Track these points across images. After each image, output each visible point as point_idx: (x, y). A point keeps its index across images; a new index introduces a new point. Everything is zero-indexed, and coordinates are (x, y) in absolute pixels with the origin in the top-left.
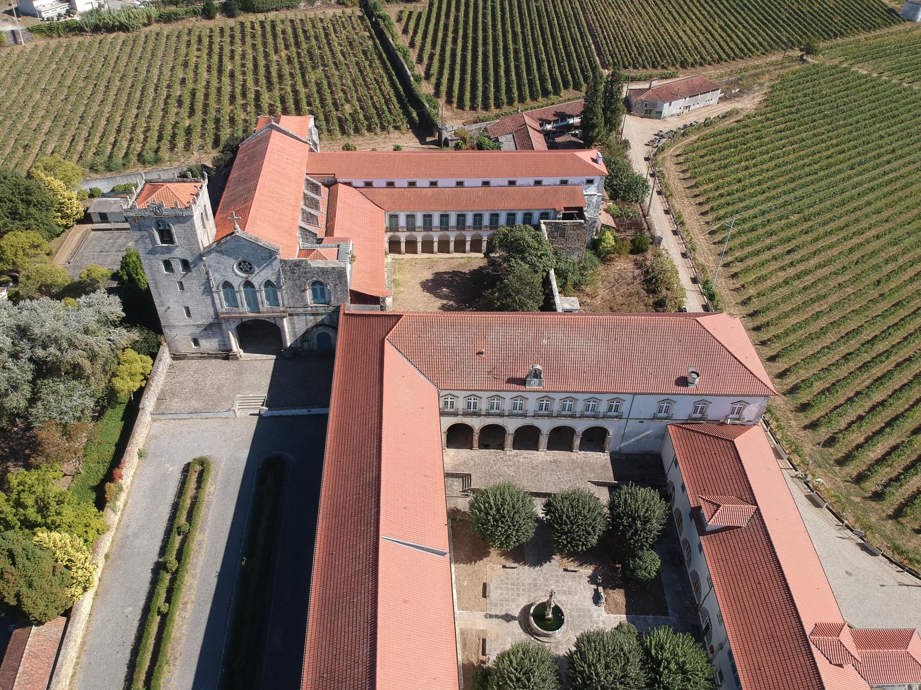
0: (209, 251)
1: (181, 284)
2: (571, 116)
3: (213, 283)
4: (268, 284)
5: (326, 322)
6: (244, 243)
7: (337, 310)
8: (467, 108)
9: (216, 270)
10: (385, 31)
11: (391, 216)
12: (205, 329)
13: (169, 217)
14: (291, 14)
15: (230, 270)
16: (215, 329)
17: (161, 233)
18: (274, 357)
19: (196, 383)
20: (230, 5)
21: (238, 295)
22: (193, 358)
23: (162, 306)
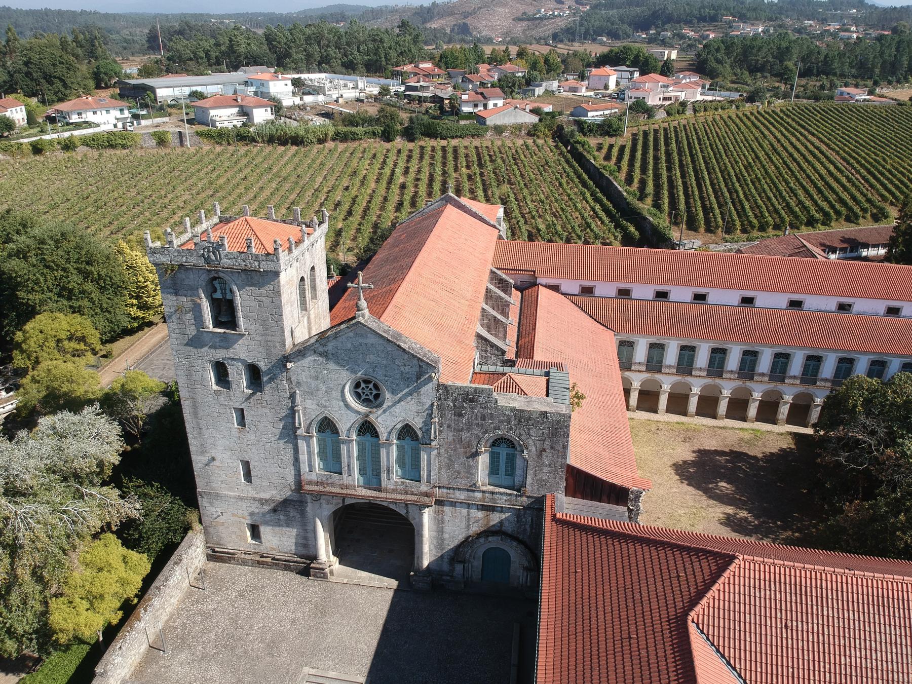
0: (301, 352)
1: (241, 413)
2: (866, 246)
3: (301, 419)
4: (406, 432)
5: (508, 528)
6: (372, 340)
7: (537, 506)
8: (702, 230)
9: (310, 393)
10: (585, 154)
11: (622, 344)
12: (274, 510)
13: (232, 271)
14: (476, 142)
15: (336, 395)
16: (293, 513)
18: (393, 583)
19: (234, 621)
20: (412, 128)
22: (244, 563)
23: (203, 453)
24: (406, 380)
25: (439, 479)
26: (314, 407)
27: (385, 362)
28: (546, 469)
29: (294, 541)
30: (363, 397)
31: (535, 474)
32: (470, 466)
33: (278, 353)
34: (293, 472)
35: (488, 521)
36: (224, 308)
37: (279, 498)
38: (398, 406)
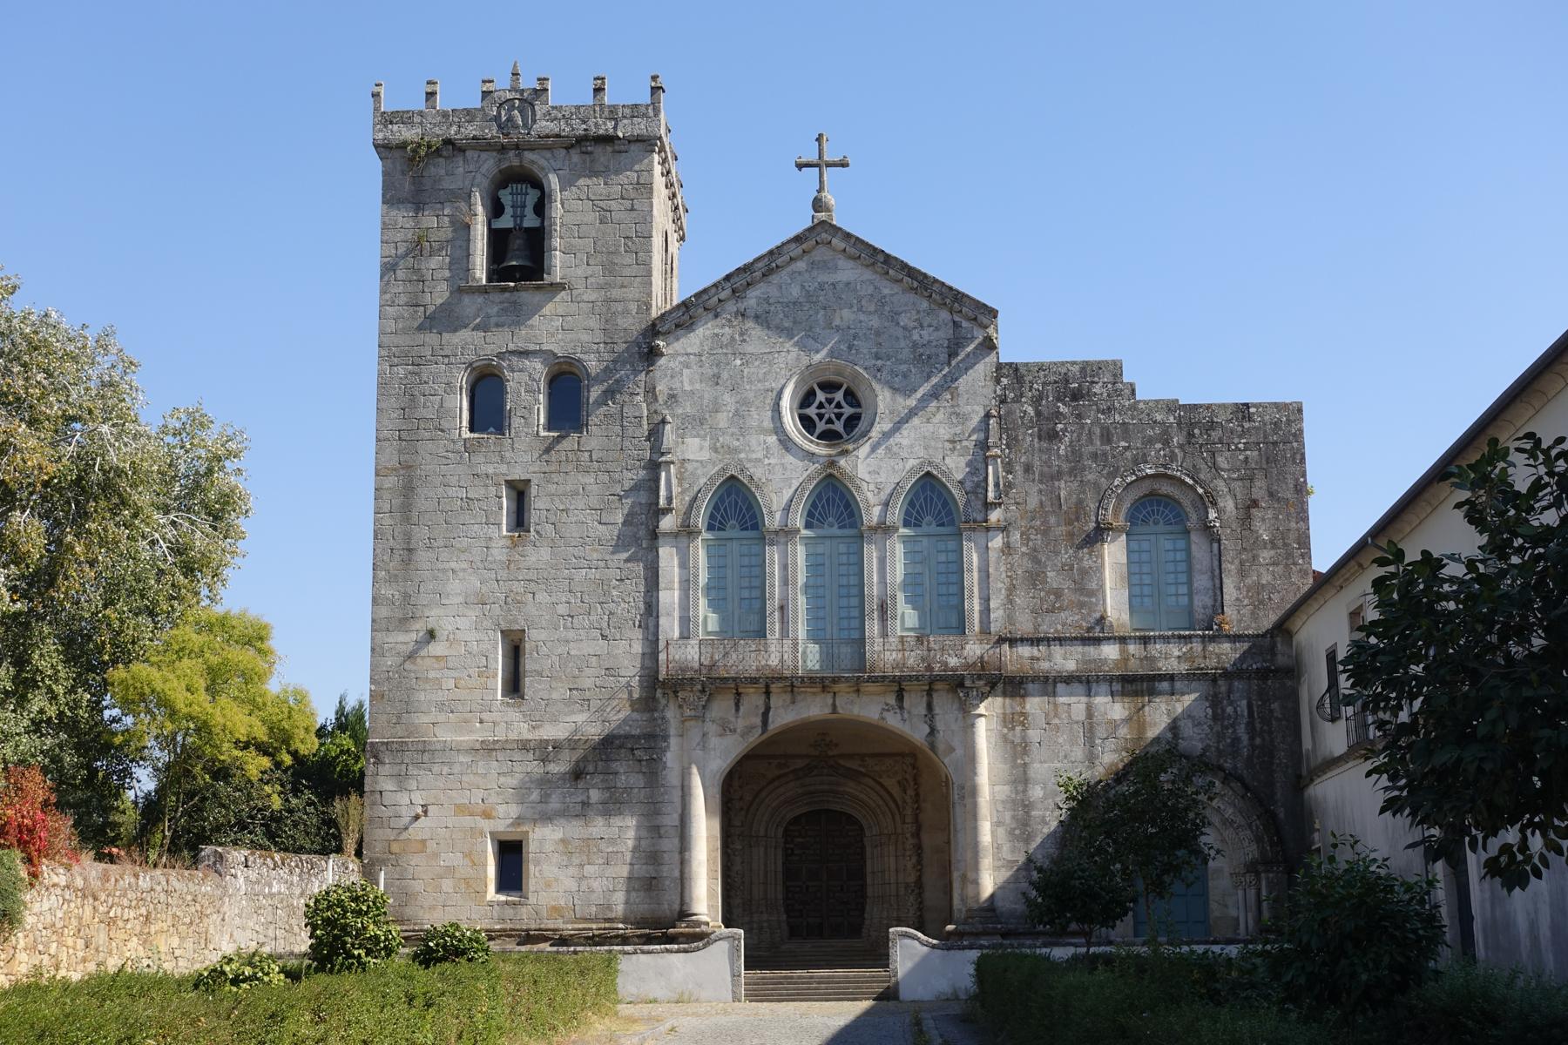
0: (686, 315)
1: (520, 493)
3: (670, 485)
4: (929, 500)
5: (1194, 740)
9: (697, 422)
12: (577, 774)
16: (628, 776)
17: (498, 241)
21: (773, 555)
24: (924, 360)
25: (1010, 619)
26: (706, 455)
27: (875, 322)
28: (1265, 555)
29: (624, 871)
30: (821, 426)
31: (1242, 573)
32: (1084, 572)
33: (632, 324)
34: (638, 648)
35: (1141, 727)
36: (517, 243)
37: (595, 731)
38: (906, 430)
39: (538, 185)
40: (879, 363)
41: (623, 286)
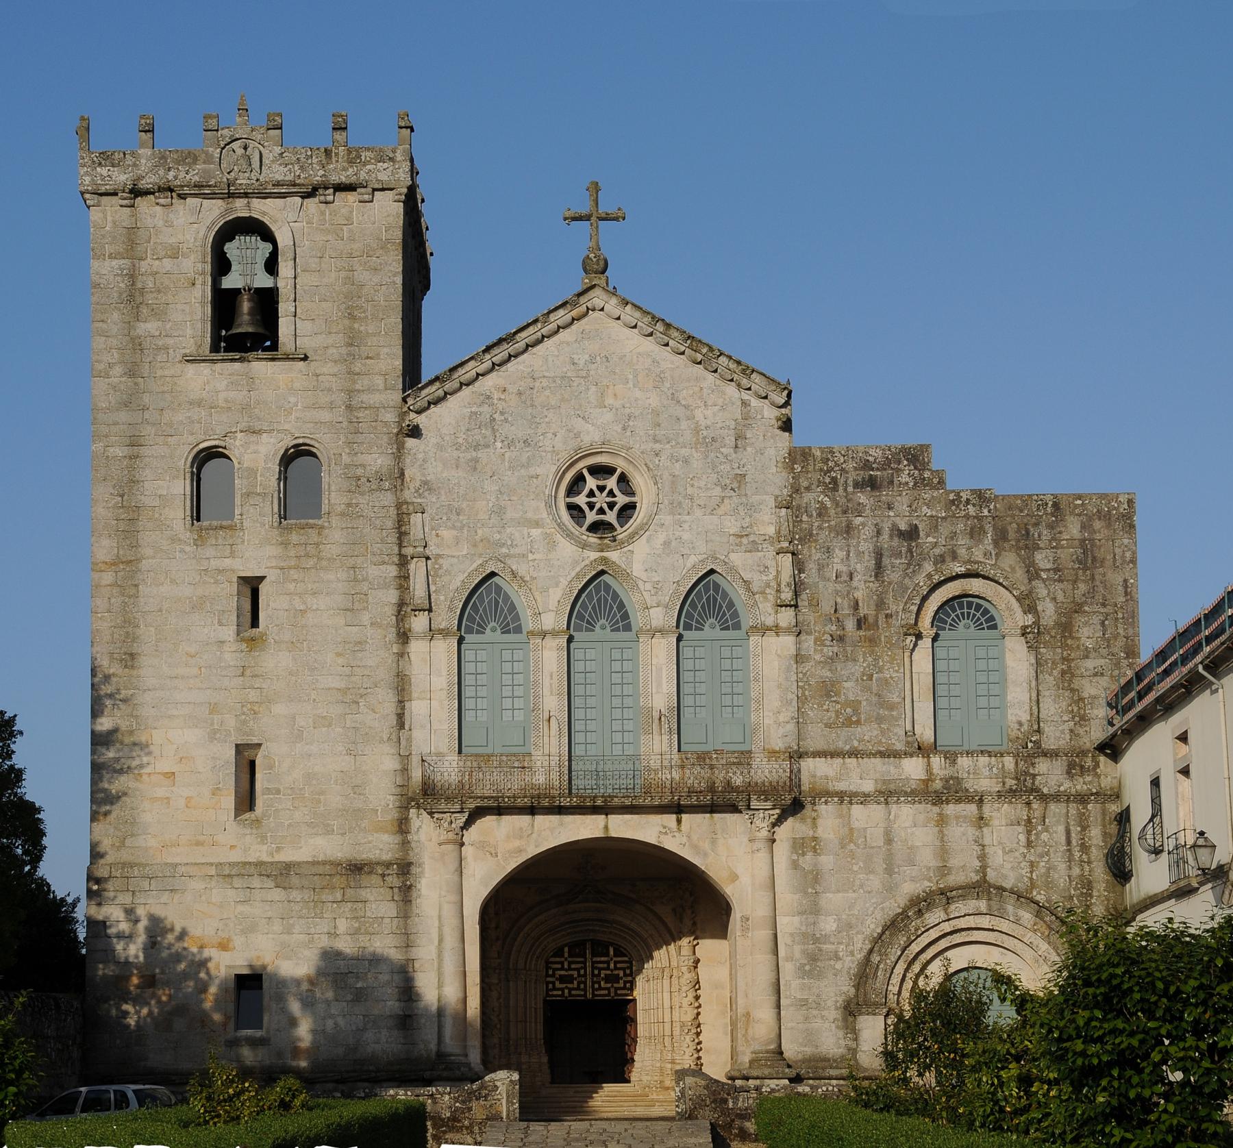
27: (654, 401)
34: (391, 763)
39: (266, 235)
40: (658, 446)
41: (368, 358)
